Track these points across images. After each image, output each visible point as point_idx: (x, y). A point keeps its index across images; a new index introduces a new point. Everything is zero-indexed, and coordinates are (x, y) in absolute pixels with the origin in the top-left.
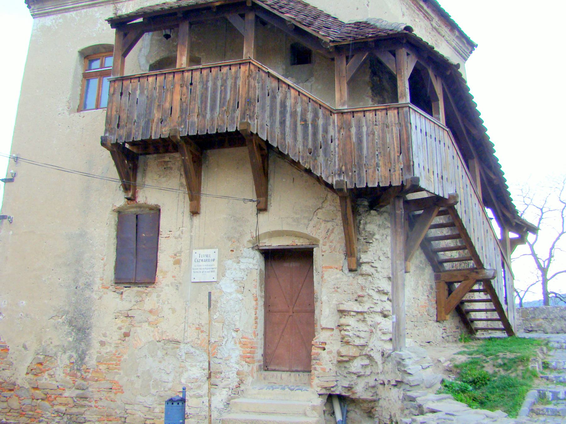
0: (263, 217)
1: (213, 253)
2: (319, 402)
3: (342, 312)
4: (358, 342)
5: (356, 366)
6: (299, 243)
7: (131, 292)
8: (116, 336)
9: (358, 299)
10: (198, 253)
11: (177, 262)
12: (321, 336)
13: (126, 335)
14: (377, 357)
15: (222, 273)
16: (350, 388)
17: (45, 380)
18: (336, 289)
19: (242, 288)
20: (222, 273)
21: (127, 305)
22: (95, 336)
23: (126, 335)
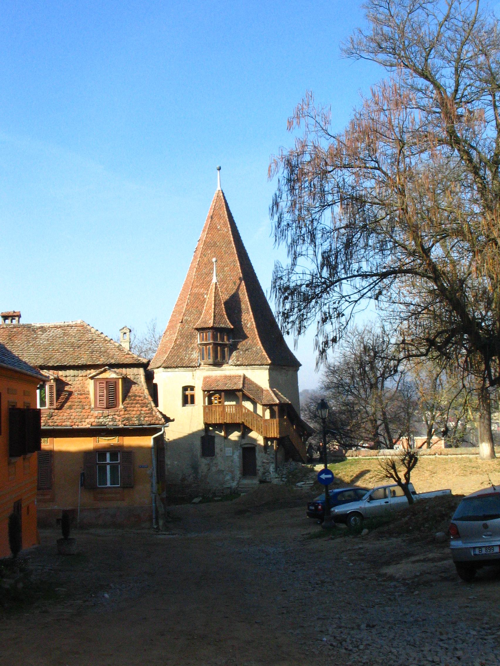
0: (243, 440)
1: (231, 449)
2: (258, 482)
3: (264, 463)
4: (267, 469)
5: (266, 474)
6: (252, 446)
7: (208, 458)
8: (206, 470)
9: (267, 459)
10: (226, 449)
11: (221, 451)
12: (258, 468)
13: (209, 469)
14: (271, 472)
15: (233, 453)
16: (265, 479)
17: (186, 482)
18: (262, 457)
19: (240, 458)
20: (233, 453)
21: (208, 462)
22: (200, 471)
23: (209, 469)
